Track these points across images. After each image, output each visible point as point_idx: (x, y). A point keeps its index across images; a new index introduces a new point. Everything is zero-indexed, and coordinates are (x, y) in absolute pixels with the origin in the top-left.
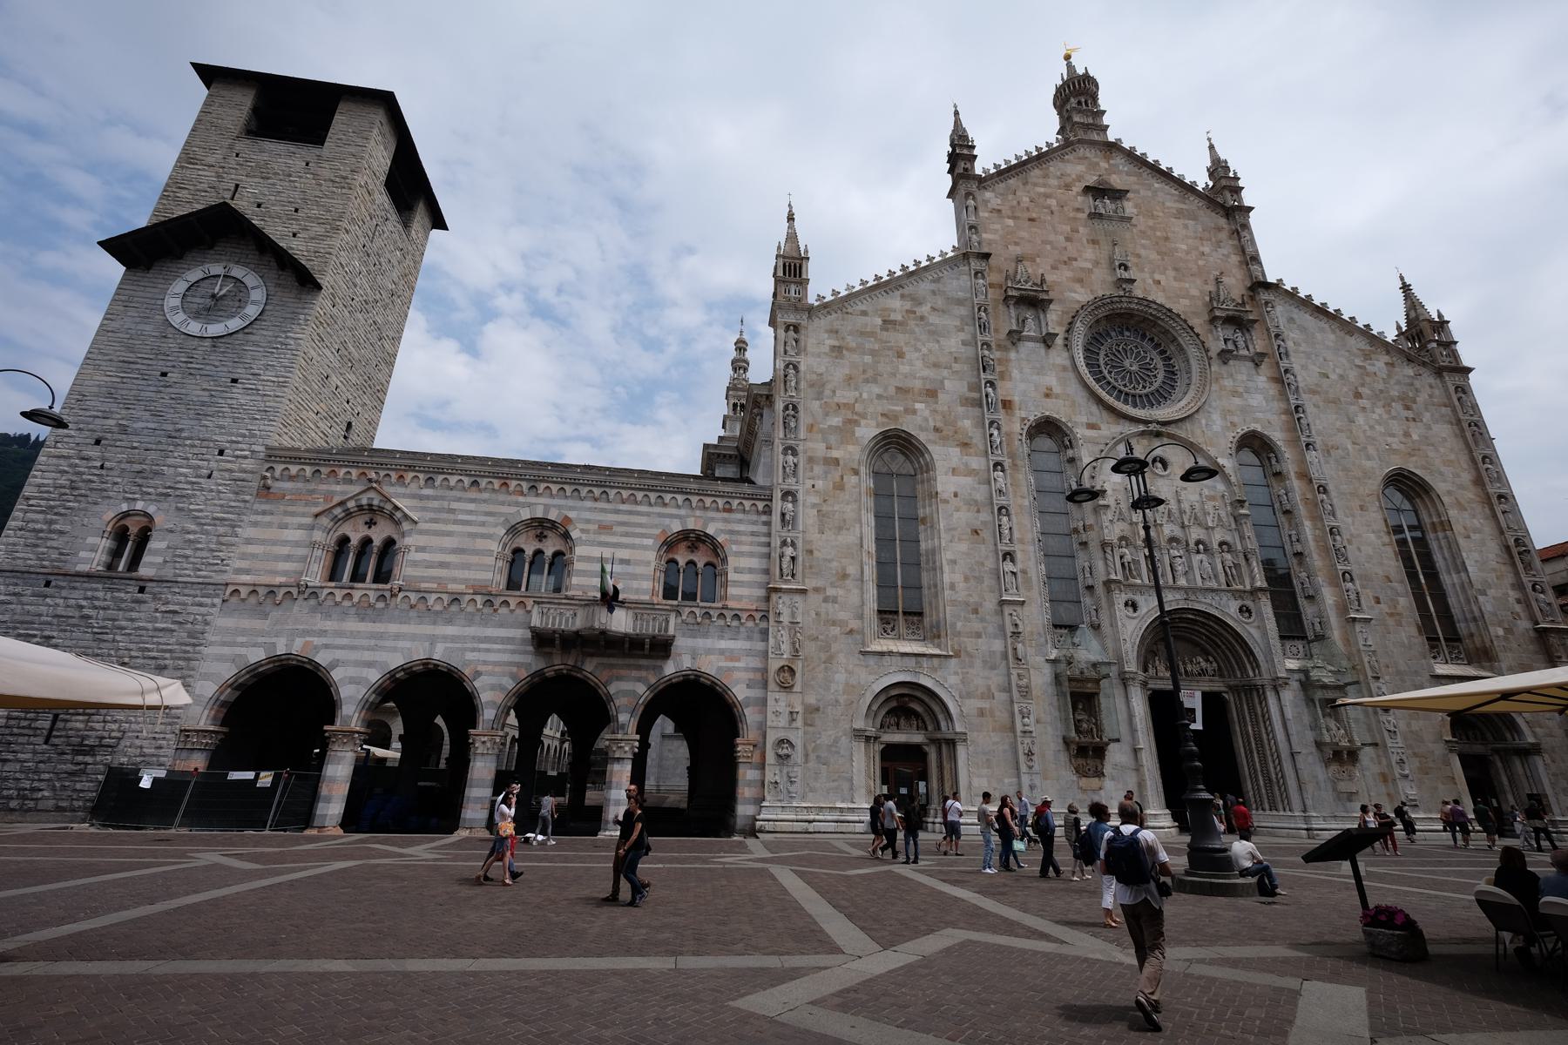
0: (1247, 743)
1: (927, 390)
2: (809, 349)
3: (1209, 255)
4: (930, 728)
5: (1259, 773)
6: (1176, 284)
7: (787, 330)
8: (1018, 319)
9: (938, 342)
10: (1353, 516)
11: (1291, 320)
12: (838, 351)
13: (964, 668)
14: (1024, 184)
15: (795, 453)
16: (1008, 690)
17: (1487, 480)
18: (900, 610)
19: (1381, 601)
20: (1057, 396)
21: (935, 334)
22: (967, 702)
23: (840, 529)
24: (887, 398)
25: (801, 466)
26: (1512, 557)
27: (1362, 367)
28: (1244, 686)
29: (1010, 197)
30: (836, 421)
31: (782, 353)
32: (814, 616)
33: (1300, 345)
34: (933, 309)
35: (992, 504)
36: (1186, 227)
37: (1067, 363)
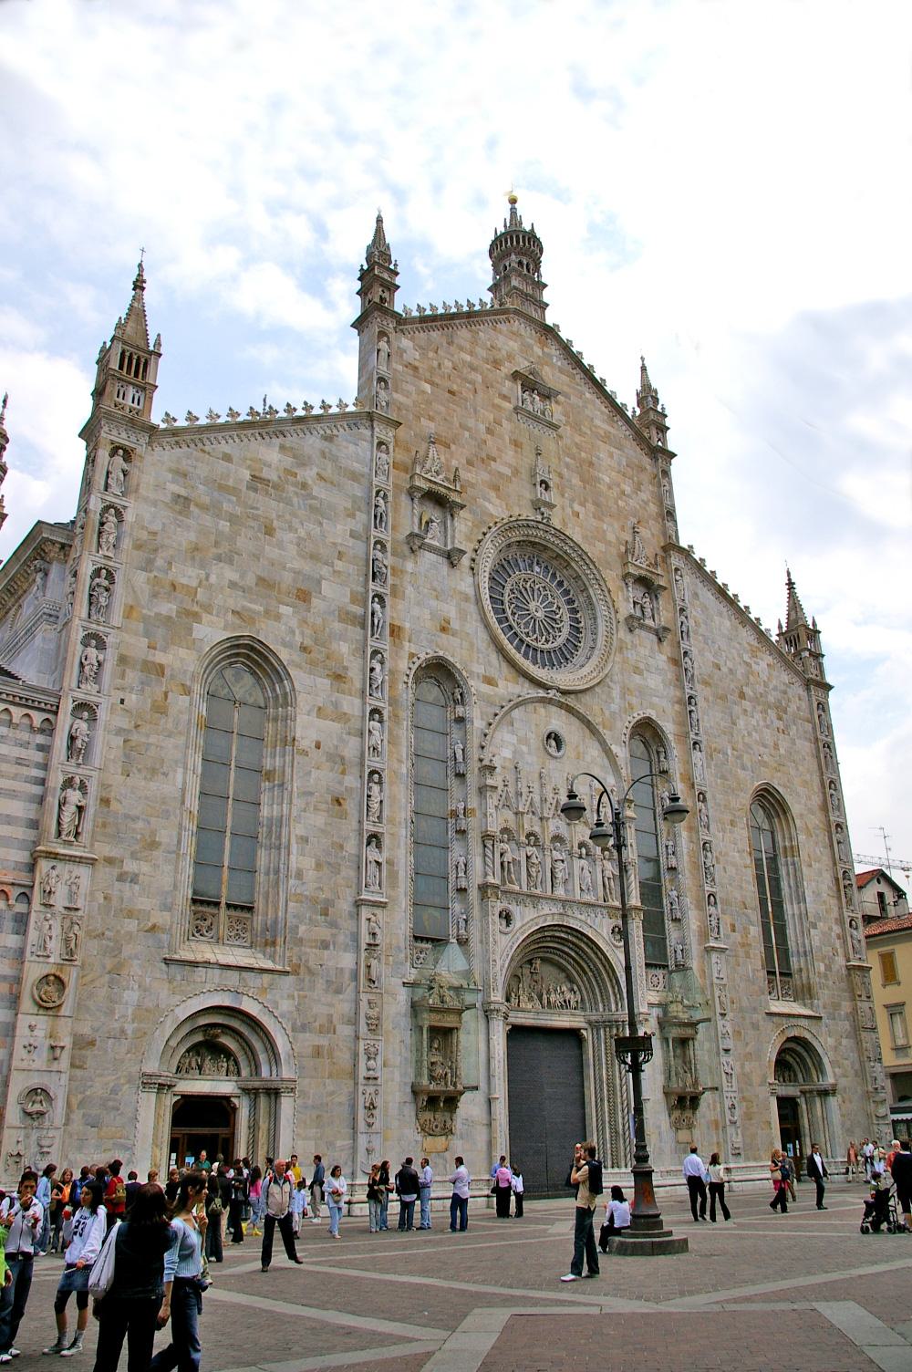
0: (599, 1091)
1: (298, 590)
2: (142, 491)
3: (628, 496)
4: (245, 1072)
5: (607, 1125)
6: (594, 522)
7: (113, 453)
8: (421, 520)
9: (321, 524)
10: (724, 831)
11: (696, 595)
12: (181, 502)
13: (302, 989)
14: (448, 343)
15: (101, 646)
16: (354, 1022)
17: (830, 806)
18: (223, 901)
19: (737, 929)
21: (319, 512)
22: (301, 1036)
23: (154, 771)
24: (244, 592)
25: (108, 667)
26: (839, 890)
27: (748, 664)
28: (604, 1022)
29: (431, 354)
30: (168, 608)
31: (102, 488)
32: (102, 901)
35: (362, 764)
36: (611, 456)
37: (471, 591)
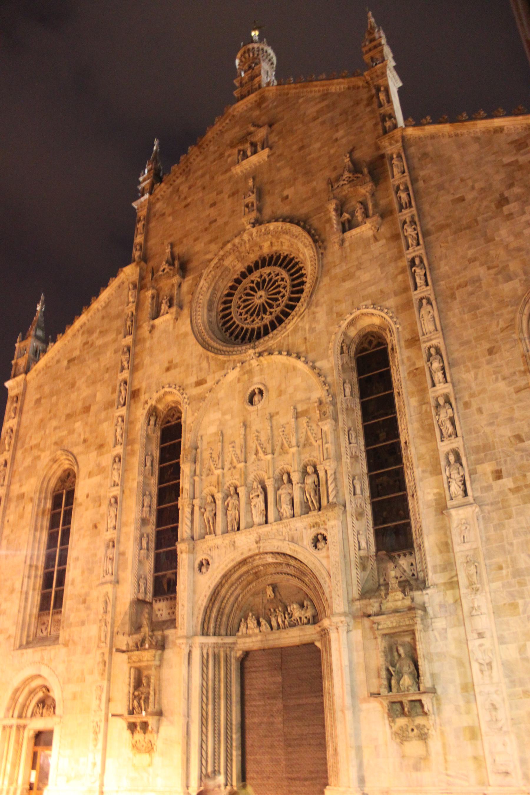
3: (342, 138)
9: (98, 360)
10: (476, 367)
12: (38, 401)
19: (504, 473)
20: (176, 366)
33: (432, 179)
34: (101, 332)
36: (323, 123)
37: (189, 328)
